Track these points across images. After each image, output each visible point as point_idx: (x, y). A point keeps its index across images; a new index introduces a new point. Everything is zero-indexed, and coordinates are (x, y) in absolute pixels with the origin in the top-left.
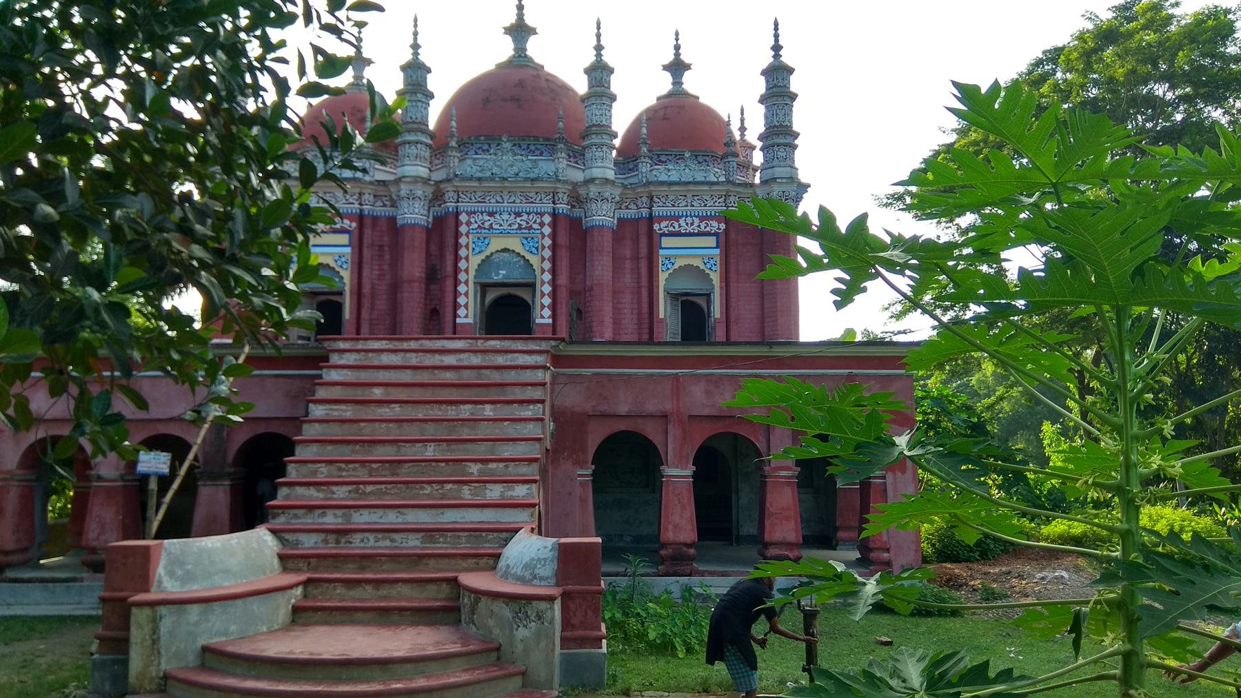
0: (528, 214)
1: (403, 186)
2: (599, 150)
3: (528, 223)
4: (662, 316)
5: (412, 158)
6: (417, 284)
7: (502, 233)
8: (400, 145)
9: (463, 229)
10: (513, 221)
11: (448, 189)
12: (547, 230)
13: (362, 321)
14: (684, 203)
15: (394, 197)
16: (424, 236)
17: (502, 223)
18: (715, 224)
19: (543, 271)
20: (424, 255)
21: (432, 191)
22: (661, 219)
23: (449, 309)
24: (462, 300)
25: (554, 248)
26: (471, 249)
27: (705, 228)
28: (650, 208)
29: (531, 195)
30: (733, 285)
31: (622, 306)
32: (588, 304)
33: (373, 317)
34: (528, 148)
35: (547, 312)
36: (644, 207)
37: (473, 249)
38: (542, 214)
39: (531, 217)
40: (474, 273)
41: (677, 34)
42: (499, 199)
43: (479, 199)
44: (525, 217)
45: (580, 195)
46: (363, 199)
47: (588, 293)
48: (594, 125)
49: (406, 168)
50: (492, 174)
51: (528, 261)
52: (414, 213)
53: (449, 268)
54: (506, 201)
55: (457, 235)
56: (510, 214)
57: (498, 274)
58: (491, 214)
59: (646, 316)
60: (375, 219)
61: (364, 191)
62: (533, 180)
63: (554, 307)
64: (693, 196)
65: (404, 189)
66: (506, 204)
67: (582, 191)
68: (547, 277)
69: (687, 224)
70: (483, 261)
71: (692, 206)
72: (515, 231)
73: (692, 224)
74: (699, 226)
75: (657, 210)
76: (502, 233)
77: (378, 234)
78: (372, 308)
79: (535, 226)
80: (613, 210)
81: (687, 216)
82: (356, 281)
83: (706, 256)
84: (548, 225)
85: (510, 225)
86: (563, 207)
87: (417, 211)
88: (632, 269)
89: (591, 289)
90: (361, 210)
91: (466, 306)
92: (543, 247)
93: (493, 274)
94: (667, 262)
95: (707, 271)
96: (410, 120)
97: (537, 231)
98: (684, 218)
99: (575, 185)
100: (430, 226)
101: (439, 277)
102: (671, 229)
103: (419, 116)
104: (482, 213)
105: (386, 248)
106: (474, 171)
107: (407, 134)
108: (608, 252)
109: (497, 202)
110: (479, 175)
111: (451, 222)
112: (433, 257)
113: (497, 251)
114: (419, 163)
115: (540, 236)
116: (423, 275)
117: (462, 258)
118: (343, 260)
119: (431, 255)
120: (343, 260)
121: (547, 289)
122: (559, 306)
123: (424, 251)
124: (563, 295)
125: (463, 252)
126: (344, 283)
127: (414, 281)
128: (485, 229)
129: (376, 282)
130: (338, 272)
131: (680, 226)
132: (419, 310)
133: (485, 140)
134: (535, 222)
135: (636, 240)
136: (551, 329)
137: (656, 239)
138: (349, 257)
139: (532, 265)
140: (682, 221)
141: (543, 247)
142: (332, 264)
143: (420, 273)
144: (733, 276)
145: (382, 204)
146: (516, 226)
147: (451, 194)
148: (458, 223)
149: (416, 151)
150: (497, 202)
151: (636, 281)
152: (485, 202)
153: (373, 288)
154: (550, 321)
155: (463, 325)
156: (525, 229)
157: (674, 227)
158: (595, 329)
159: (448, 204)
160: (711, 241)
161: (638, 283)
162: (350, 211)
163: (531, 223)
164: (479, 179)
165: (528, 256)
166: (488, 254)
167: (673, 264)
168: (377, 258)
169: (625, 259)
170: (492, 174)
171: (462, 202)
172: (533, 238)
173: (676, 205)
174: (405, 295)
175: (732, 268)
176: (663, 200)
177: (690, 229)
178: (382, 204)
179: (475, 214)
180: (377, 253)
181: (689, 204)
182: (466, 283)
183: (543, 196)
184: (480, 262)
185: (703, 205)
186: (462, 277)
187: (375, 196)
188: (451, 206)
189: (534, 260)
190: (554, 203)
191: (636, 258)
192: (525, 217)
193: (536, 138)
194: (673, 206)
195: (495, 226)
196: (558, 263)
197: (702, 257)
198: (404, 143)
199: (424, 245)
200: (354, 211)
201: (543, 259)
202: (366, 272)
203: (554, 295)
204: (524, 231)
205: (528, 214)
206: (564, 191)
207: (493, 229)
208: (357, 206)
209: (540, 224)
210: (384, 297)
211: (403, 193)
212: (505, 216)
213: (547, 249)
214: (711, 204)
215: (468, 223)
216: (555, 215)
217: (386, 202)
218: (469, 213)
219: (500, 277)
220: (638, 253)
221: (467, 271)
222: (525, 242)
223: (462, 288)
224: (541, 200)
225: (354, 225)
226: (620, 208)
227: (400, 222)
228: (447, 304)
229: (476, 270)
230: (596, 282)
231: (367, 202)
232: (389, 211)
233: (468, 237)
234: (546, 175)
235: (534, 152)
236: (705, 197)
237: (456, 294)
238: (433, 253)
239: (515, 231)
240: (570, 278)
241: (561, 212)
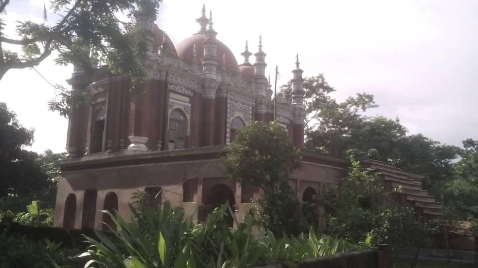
9: (228, 105)
41: (247, 41)
52: (212, 95)
55: (226, 108)
58: (236, 102)
125: (228, 115)
138: (190, 108)
142: (184, 110)
146: (242, 108)
148: (226, 103)
186: (228, 125)
192: (245, 105)
212: (240, 104)
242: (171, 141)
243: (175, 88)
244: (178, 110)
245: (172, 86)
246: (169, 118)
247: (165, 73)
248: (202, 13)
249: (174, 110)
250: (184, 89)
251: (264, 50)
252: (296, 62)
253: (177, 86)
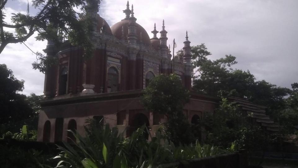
9: (144, 64)
41: (155, 24)
58: (149, 62)
125: (144, 70)
138: (120, 66)
142: (116, 67)
186: (144, 77)
192: (154, 64)
212: (151, 63)
218: (145, 61)
243: (111, 54)
244: (113, 68)
245: (109, 53)
246: (107, 72)
247: (104, 44)
248: (126, 7)
249: (110, 67)
250: (116, 55)
251: (166, 29)
252: (186, 36)
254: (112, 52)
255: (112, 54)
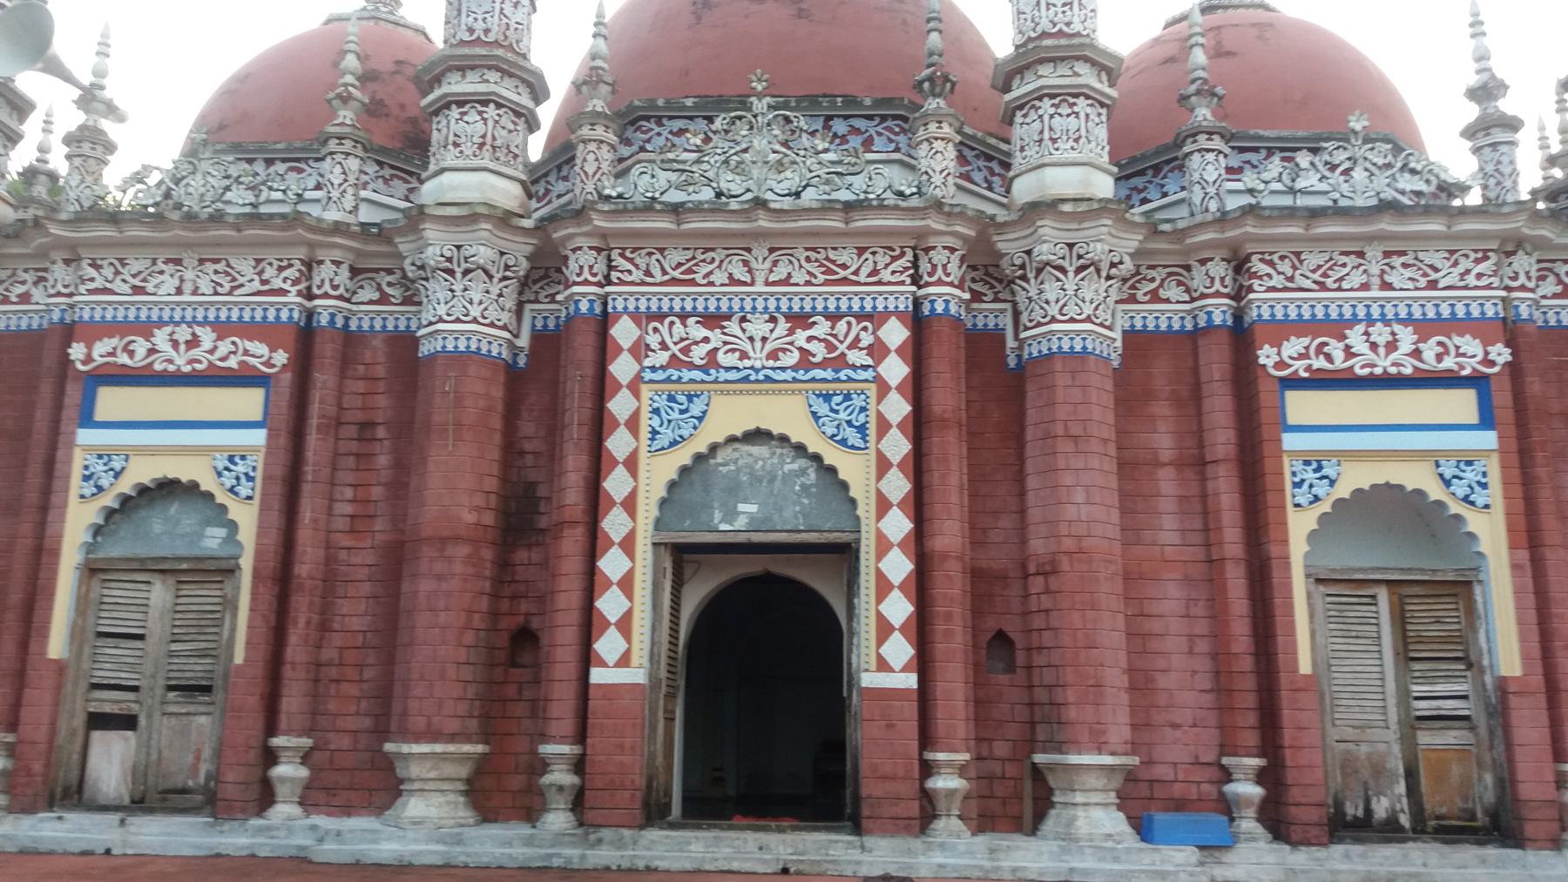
0: (834, 318)
1: (431, 232)
2: (1065, 110)
3: (831, 347)
4: (1305, 666)
5: (468, 149)
6: (462, 551)
7: (746, 379)
8: (436, 113)
9: (623, 368)
10: (777, 344)
11: (579, 242)
12: (896, 370)
13: (287, 672)
14: (1357, 279)
15: (411, 272)
16: (498, 392)
17: (747, 346)
18: (1471, 346)
19: (883, 506)
20: (495, 454)
21: (529, 249)
22: (1283, 329)
23: (565, 635)
24: (610, 604)
25: (918, 426)
26: (644, 433)
27: (1439, 358)
28: (1238, 296)
29: (843, 257)
30: (1552, 557)
31: (1155, 626)
32: (1038, 622)
33: (328, 654)
34: (827, 127)
35: (900, 650)
36: (1217, 294)
37: (654, 432)
38: (876, 318)
39: (841, 326)
40: (655, 512)
42: (740, 273)
43: (676, 274)
44: (822, 328)
45: (1003, 255)
46: (316, 281)
47: (1037, 584)
48: (1044, 35)
49: (447, 178)
50: (719, 195)
51: (832, 470)
53: (573, 496)
54: (760, 279)
55: (602, 387)
56: (773, 320)
57: (731, 515)
58: (713, 320)
59: (1247, 663)
60: (350, 340)
61: (320, 254)
62: (849, 207)
63: (922, 630)
64: (1387, 254)
65: (436, 244)
66: (759, 287)
67: (1009, 246)
68: (898, 525)
69: (1374, 346)
70: (684, 470)
71: (1386, 286)
72: (788, 375)
73: (1392, 346)
74: (1416, 354)
75: (1264, 303)
76: (746, 379)
77: (360, 386)
78: (324, 627)
79: (855, 357)
80: (1114, 296)
81: (1370, 322)
82: (273, 538)
83: (1447, 453)
84: (900, 351)
85: (773, 355)
86: (945, 297)
87: (475, 311)
88: (1182, 499)
89: (1050, 570)
90: (310, 314)
91: (625, 625)
92: (884, 426)
93: (717, 516)
94: (1310, 475)
95: (1455, 508)
96: (467, 37)
97: (862, 375)
98: (1360, 328)
99: (987, 225)
100: (522, 361)
101: (543, 522)
102: (1320, 363)
103: (494, 22)
104: (683, 317)
105: (381, 432)
106: (663, 184)
107: (455, 77)
108: (1105, 441)
109: (733, 281)
110: (675, 196)
111: (583, 347)
112: (529, 460)
113: (732, 440)
114: (491, 165)
115: (872, 390)
116: (489, 519)
117: (615, 463)
118: (240, 468)
119: (522, 453)
120: (240, 468)
121: (899, 566)
122: (939, 627)
123: (498, 438)
124: (951, 589)
125: (618, 443)
126: (239, 544)
127: (456, 539)
128: (692, 366)
129: (346, 542)
130: (223, 509)
131: (1349, 353)
132: (469, 637)
133: (696, 107)
134: (854, 345)
135: (1192, 399)
136: (911, 710)
137: (1266, 396)
138: (258, 460)
139: (844, 486)
140: (1355, 338)
141: (884, 426)
142: (208, 483)
143: (478, 509)
144: (1549, 523)
145: (376, 296)
146: (793, 358)
147: (587, 257)
148: (604, 349)
149: (480, 125)
150: (733, 281)
151: (1197, 538)
152: (693, 282)
153: (330, 561)
154: (911, 681)
155: (612, 690)
156: (822, 365)
157: (1329, 358)
158: (1072, 713)
159: (576, 289)
160: (1461, 404)
161: (1208, 545)
162: (271, 316)
163: (842, 348)
164: (676, 210)
165: (832, 456)
166: (703, 449)
167: (1332, 483)
168: (351, 462)
169: (1158, 464)
170: (719, 195)
171: (622, 282)
172: (848, 397)
173: (1329, 282)
174: (426, 586)
175: (1545, 495)
176: (1286, 267)
177: (1384, 364)
178: (376, 296)
179: (660, 317)
180: (354, 446)
181: (1376, 281)
182: (628, 545)
183: (882, 260)
184: (674, 476)
185: (1423, 282)
186: (614, 524)
187: (355, 271)
188: (584, 295)
189: (853, 469)
190: (916, 280)
191: (1196, 462)
192: (822, 328)
193: (851, 101)
194: (1322, 287)
195: (722, 358)
196: (934, 478)
197: (1434, 457)
198: (446, 104)
199: (497, 422)
200: (284, 315)
201: (883, 465)
202: (308, 512)
203: (921, 587)
204: (818, 373)
205: (834, 318)
206: (950, 241)
207: (718, 366)
208: (292, 298)
209: (870, 350)
210: (366, 588)
211: (432, 255)
212: (758, 327)
213: (894, 433)
214: (1453, 279)
215: (639, 350)
216: (918, 321)
217: (389, 291)
219: (741, 523)
220: (1201, 445)
221: (630, 504)
222: (823, 409)
223: (612, 564)
224: (874, 272)
225: (281, 358)
226: (1132, 299)
227: (425, 349)
228: (560, 618)
229: (663, 503)
230: (1068, 544)
231: (327, 288)
232: (394, 318)
233: (636, 394)
234: (888, 194)
235: (844, 139)
236: (1428, 258)
237: (592, 583)
238: (528, 446)
239: (788, 375)
240: (973, 527)
241: (940, 308)
242: (99, 721)
245: (101, 348)
250: (207, 337)
253: (148, 336)
254: (145, 329)
255: (141, 347)
